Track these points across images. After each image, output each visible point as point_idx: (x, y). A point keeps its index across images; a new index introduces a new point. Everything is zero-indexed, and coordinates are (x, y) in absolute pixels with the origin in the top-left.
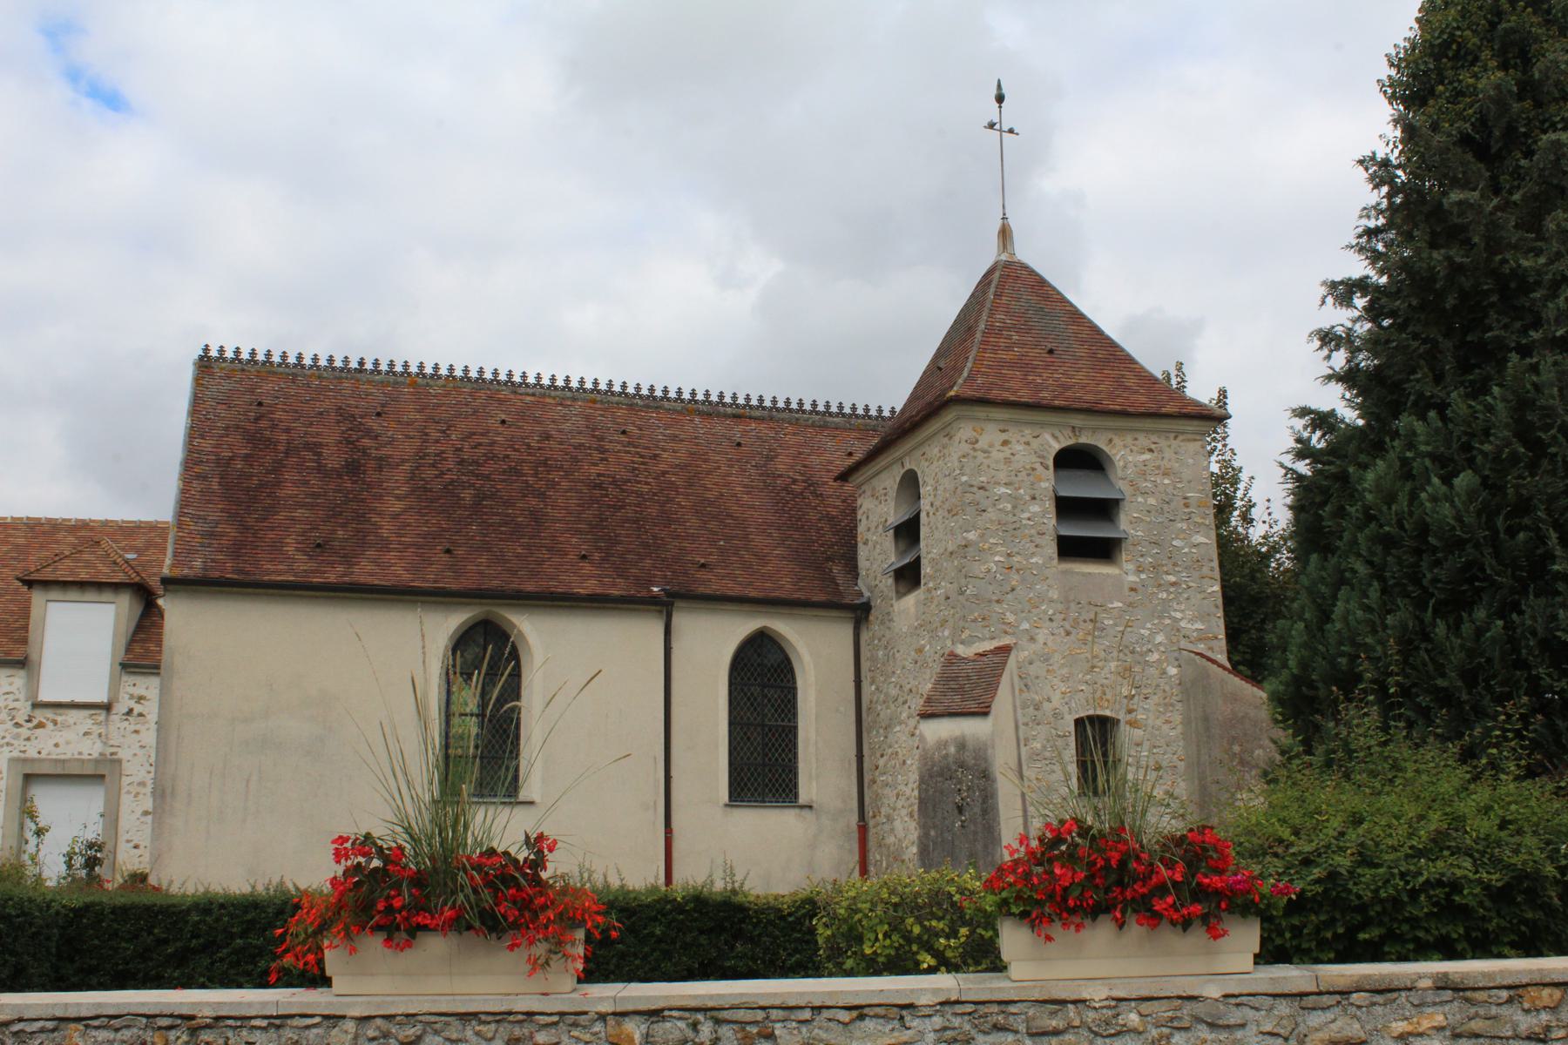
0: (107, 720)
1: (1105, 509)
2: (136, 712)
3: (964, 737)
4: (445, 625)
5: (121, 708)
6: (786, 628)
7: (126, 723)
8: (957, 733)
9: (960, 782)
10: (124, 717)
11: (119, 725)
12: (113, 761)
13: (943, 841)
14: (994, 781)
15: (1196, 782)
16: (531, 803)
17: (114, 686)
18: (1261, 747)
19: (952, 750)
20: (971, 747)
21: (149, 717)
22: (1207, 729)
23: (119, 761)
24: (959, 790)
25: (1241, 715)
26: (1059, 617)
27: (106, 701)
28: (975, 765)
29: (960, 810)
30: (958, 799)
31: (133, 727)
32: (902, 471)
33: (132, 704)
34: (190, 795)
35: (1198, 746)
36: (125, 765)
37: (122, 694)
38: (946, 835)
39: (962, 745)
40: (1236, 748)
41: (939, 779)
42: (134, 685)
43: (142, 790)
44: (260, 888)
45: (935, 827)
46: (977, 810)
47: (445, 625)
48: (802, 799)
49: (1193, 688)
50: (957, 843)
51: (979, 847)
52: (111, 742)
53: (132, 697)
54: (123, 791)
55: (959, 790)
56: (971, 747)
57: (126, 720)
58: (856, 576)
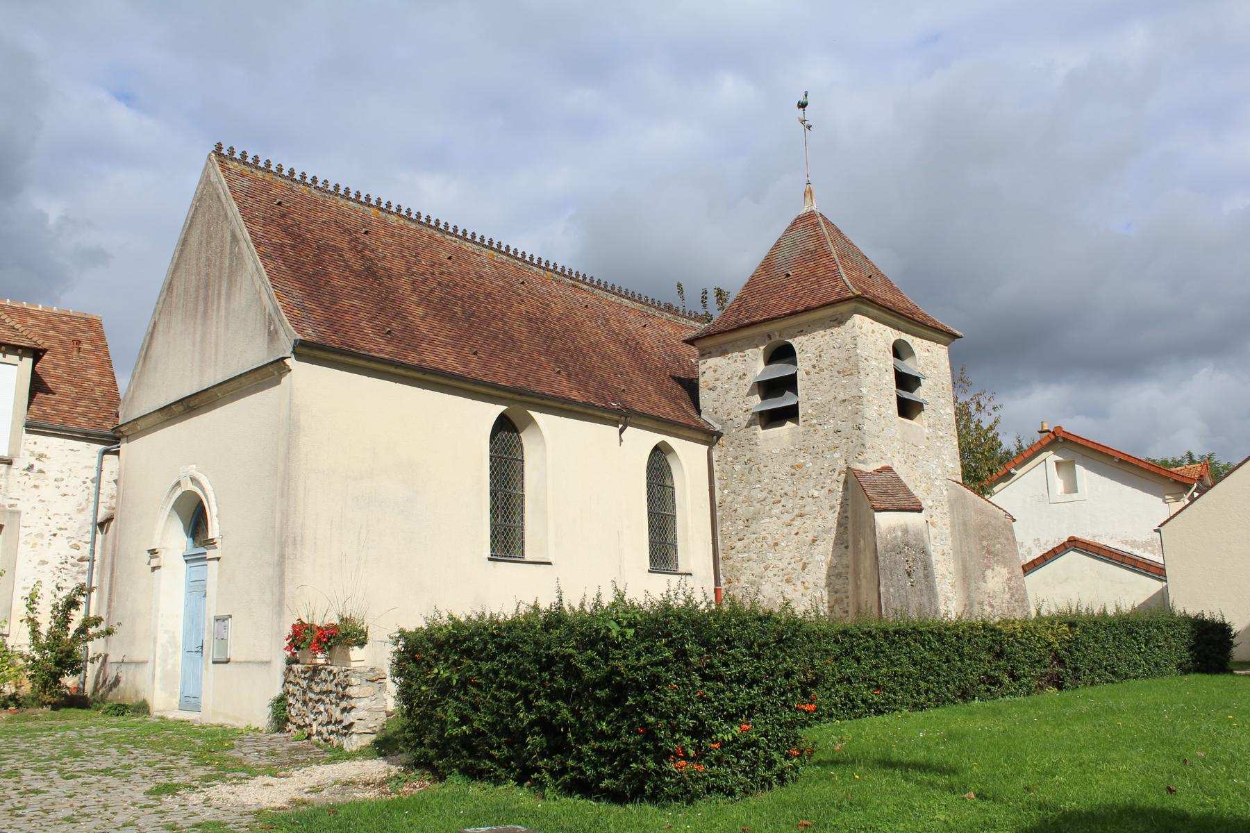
0: (7, 473)
1: (789, 383)
2: (36, 469)
3: (906, 525)
4: (494, 411)
5: (20, 464)
6: (672, 441)
7: (26, 478)
8: (902, 522)
9: (907, 556)
10: (25, 472)
11: (19, 479)
12: (12, 512)
13: (899, 596)
14: (930, 555)
15: (960, 564)
16: (549, 563)
17: (14, 442)
18: (999, 543)
19: (899, 533)
20: (912, 533)
21: (48, 474)
22: (966, 531)
23: (18, 513)
24: (907, 561)
25: (986, 522)
26: (901, 451)
27: (6, 455)
28: (916, 544)
29: (909, 575)
30: (907, 567)
31: (33, 483)
32: (768, 342)
33: (33, 461)
34: (315, 543)
35: (960, 540)
36: (23, 516)
37: (22, 451)
38: (901, 591)
39: (905, 531)
40: (985, 543)
41: (893, 553)
42: (35, 443)
43: (39, 541)
44: (1111, 611)
45: (893, 586)
46: (921, 575)
47: (494, 411)
48: (680, 570)
49: (955, 505)
50: (909, 597)
51: (925, 599)
52: (11, 495)
53: (32, 454)
54: (20, 541)
55: (907, 561)
56: (912, 533)
57: (26, 475)
58: (699, 412)
